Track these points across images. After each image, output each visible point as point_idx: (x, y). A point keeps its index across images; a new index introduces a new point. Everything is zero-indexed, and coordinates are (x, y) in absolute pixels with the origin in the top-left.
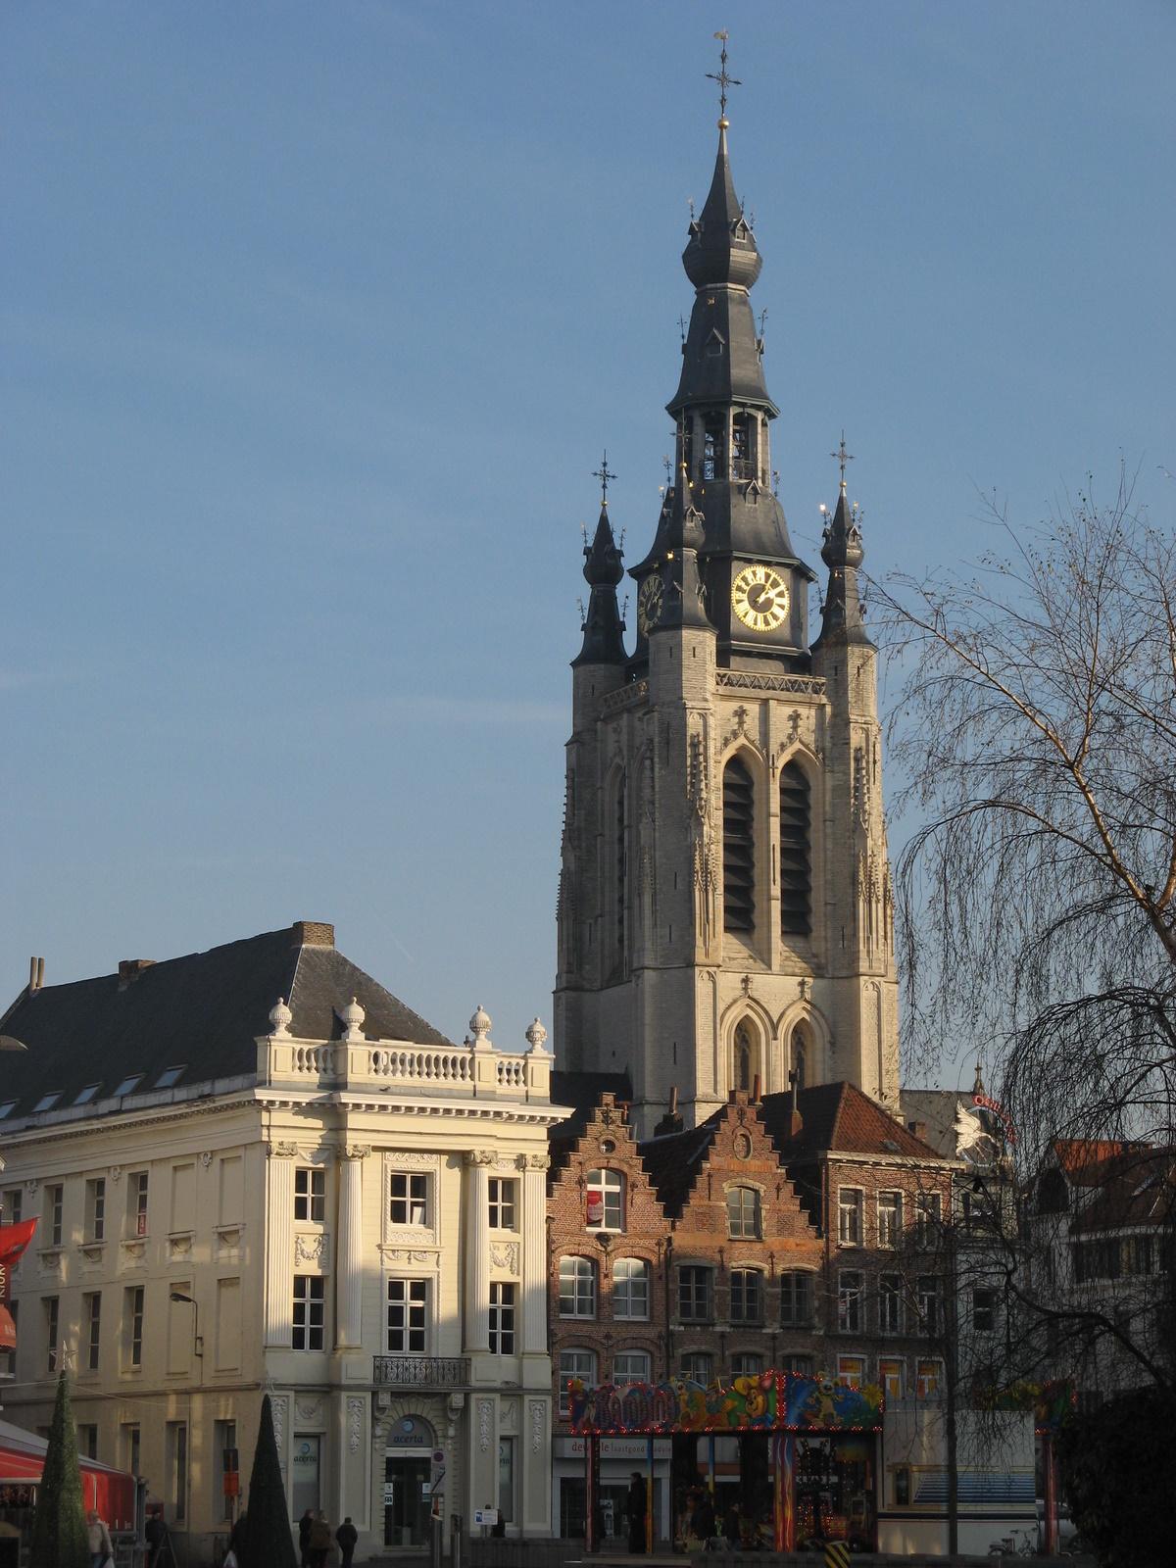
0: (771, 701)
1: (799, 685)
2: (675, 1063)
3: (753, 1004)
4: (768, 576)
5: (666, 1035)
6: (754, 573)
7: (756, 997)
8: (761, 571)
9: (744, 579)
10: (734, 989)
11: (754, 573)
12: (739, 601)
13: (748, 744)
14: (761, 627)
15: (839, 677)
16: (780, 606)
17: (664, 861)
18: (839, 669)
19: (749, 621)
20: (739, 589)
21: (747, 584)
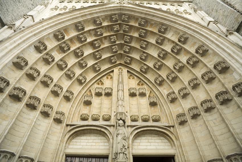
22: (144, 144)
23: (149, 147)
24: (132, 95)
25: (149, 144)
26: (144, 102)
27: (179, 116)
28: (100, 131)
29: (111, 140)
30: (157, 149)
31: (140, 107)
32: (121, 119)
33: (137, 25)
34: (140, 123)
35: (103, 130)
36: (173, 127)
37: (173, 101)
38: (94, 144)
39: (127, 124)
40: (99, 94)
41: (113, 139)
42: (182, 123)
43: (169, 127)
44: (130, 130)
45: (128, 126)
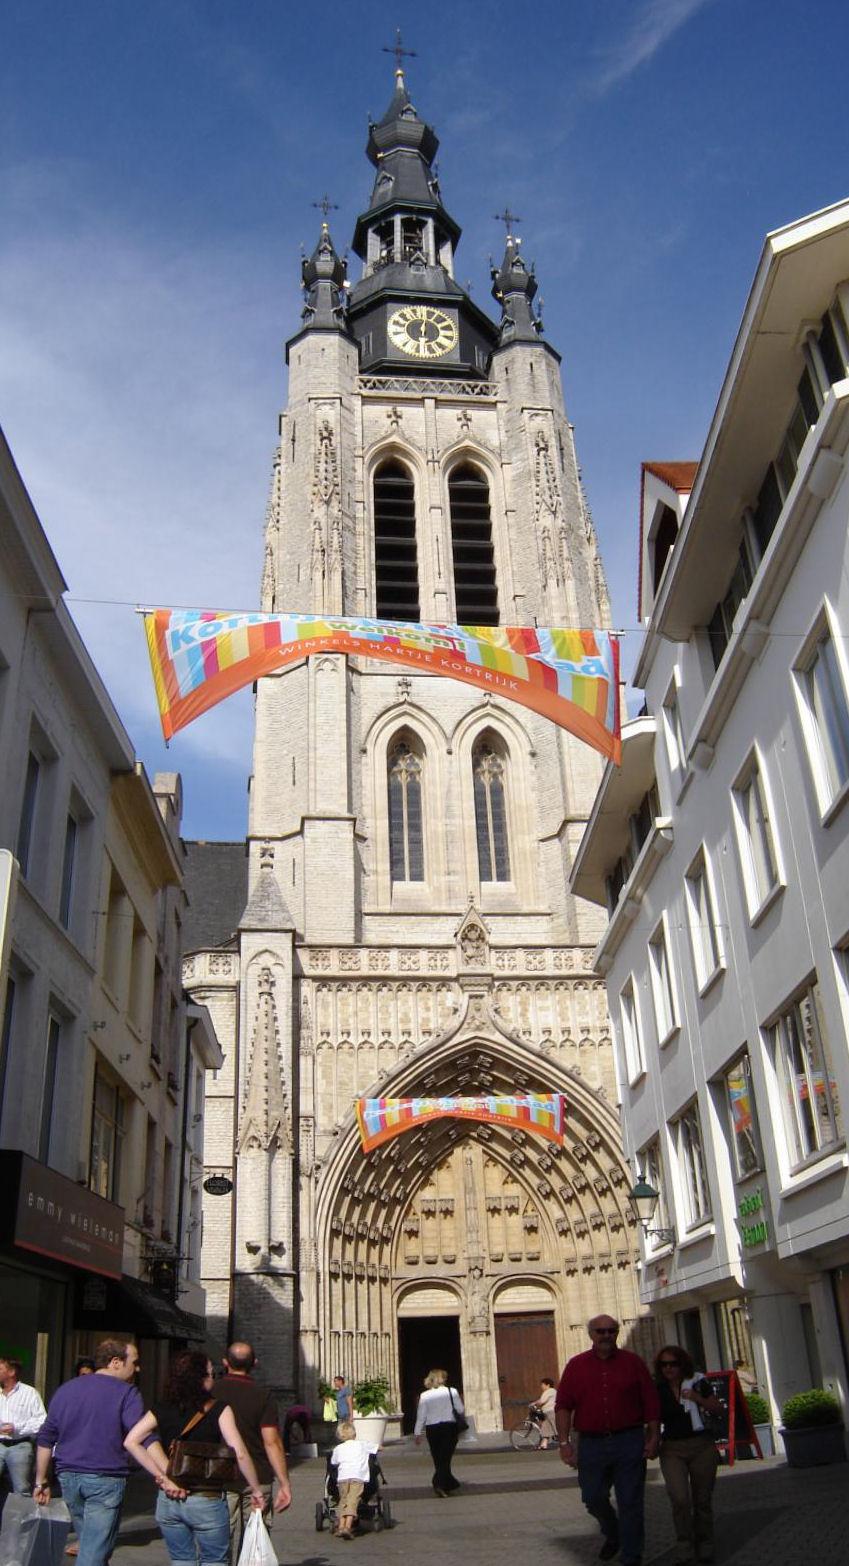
0: (426, 400)
1: (464, 388)
2: (294, 783)
3: (414, 711)
4: (430, 315)
5: (285, 752)
6: (414, 311)
7: (418, 704)
8: (422, 310)
9: (403, 316)
10: (383, 694)
11: (414, 311)
12: (396, 333)
13: (402, 442)
14: (424, 354)
15: (510, 376)
16: (446, 337)
17: (288, 557)
18: (509, 368)
19: (409, 349)
20: (396, 323)
21: (406, 320)
22: (512, 1296)
23: (518, 1301)
24: (495, 1211)
25: (517, 1296)
26: (516, 1221)
27: (568, 1261)
28: (444, 1284)
29: (464, 1298)
30: (531, 1303)
31: (506, 1235)
32: (476, 1268)
33: (512, 1082)
34: (507, 1268)
35: (448, 1283)
36: (558, 1272)
37: (564, 1233)
38: (434, 1300)
39: (485, 1273)
40: (429, 1213)
41: (466, 1295)
42: (571, 1272)
43: (552, 1273)
44: (490, 1281)
45: (487, 1276)
